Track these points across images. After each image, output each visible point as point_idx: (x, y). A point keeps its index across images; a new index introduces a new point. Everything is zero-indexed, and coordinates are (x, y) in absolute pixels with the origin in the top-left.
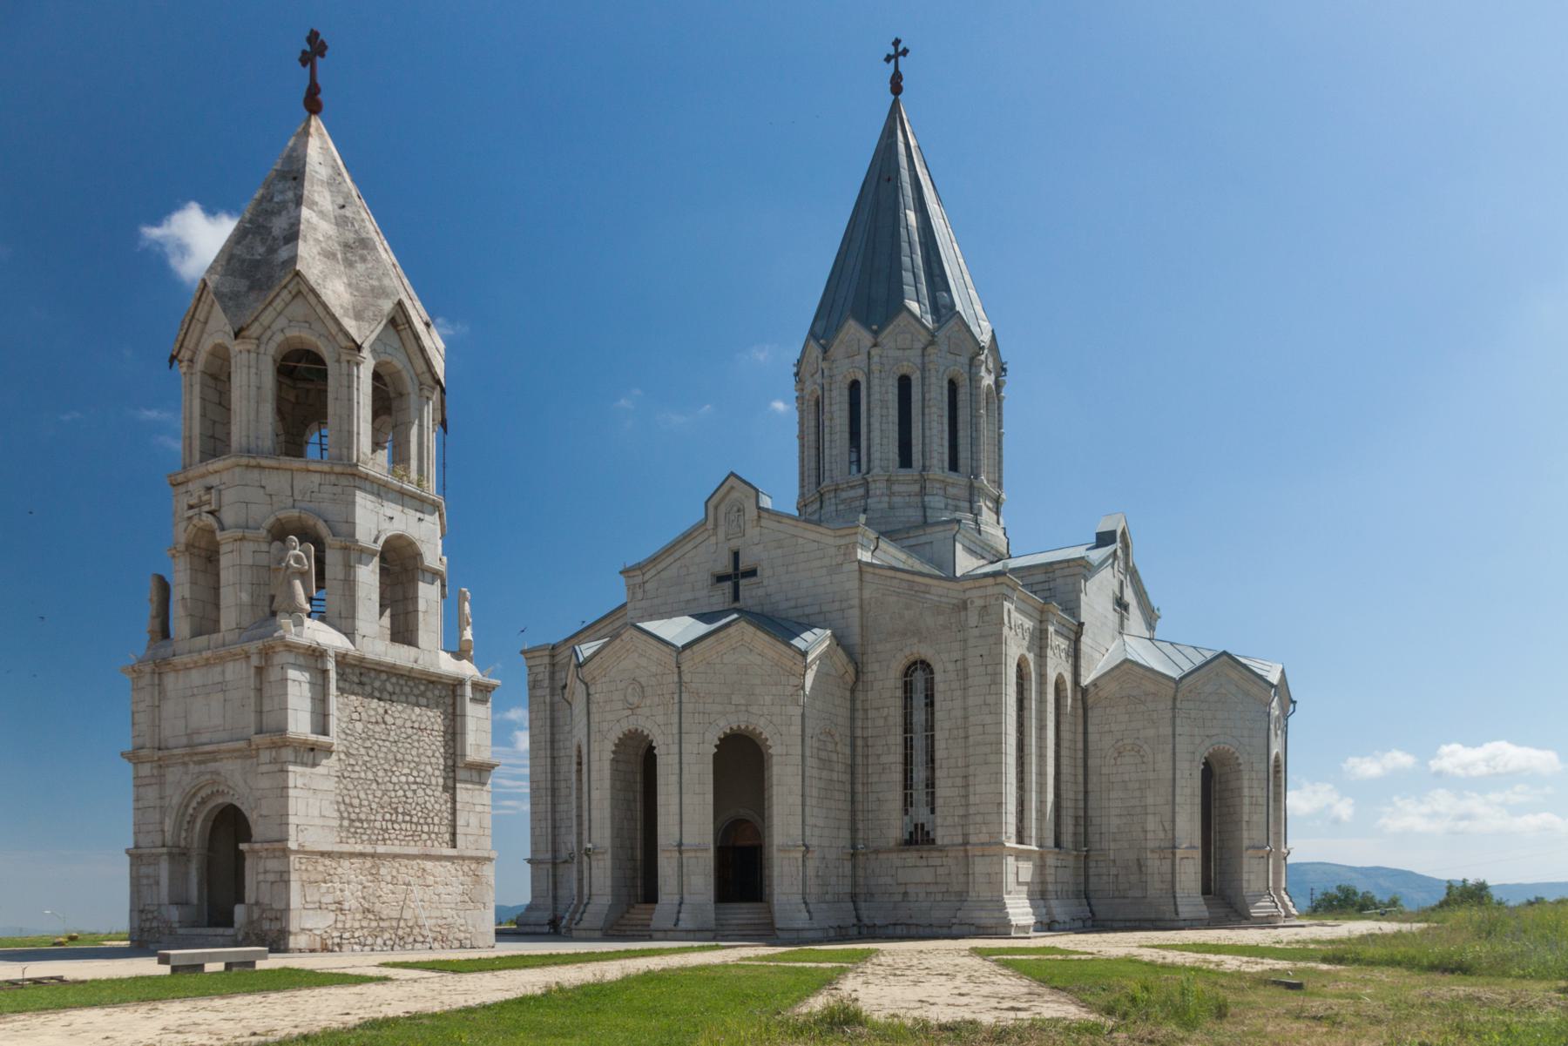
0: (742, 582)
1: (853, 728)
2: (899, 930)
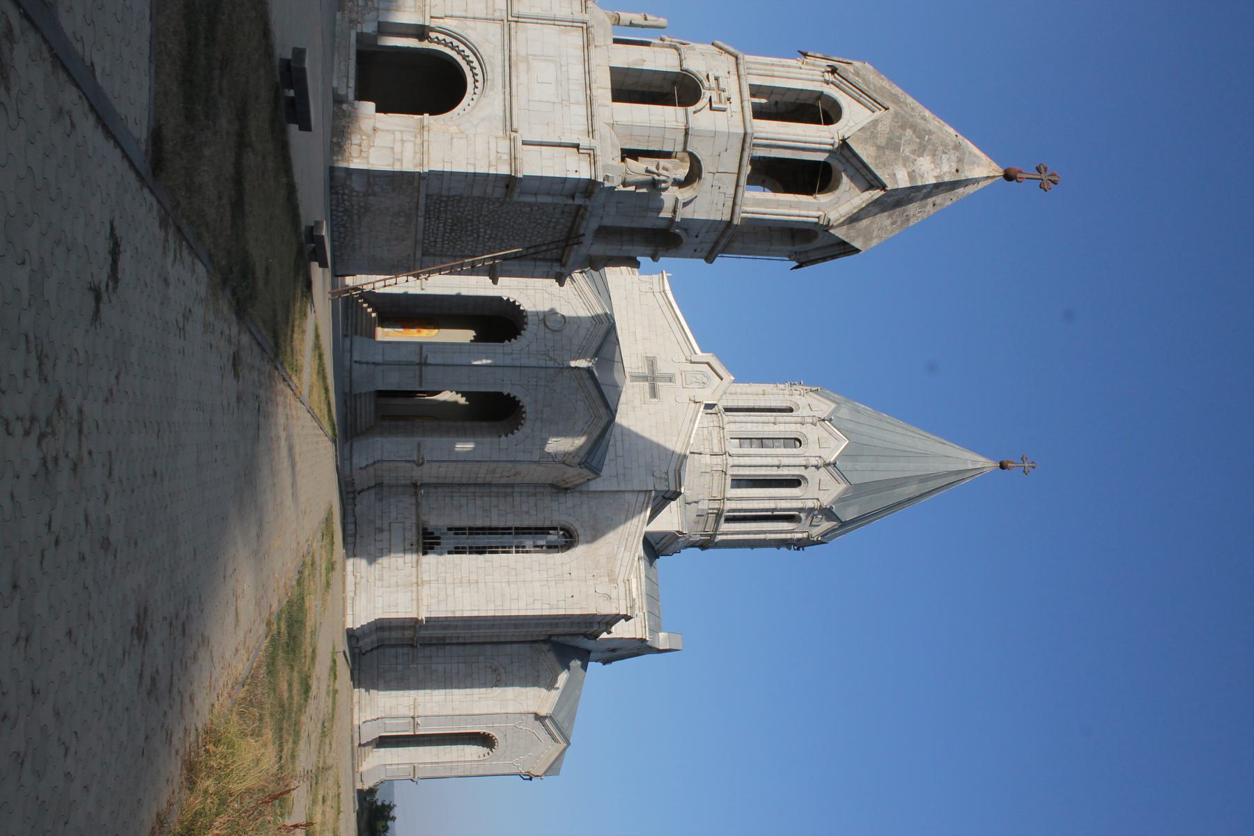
1: (521, 485)
2: (351, 527)
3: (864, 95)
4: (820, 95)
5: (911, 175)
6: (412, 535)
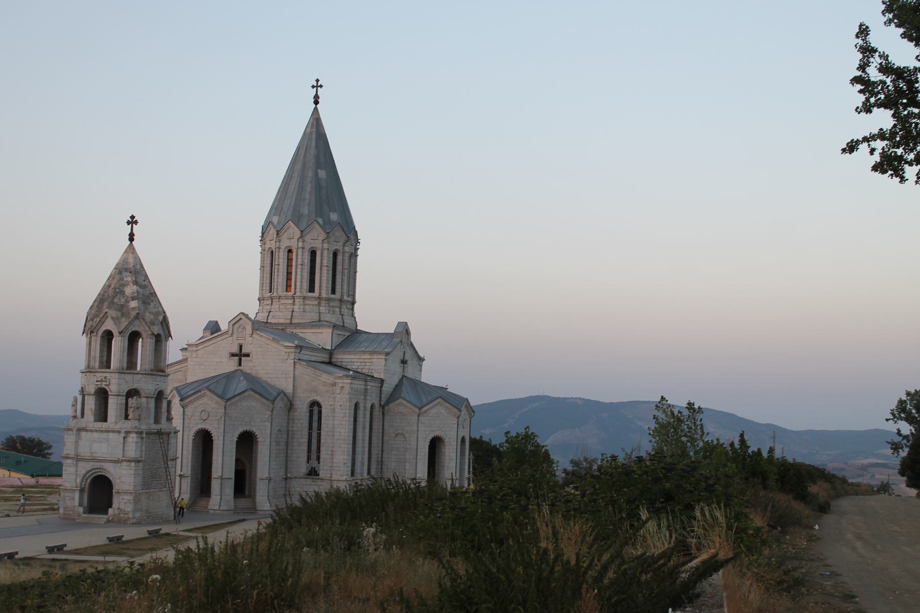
0: (243, 358)
1: (288, 427)
3: (102, 322)
4: (102, 337)
5: (133, 299)
6: (309, 481)
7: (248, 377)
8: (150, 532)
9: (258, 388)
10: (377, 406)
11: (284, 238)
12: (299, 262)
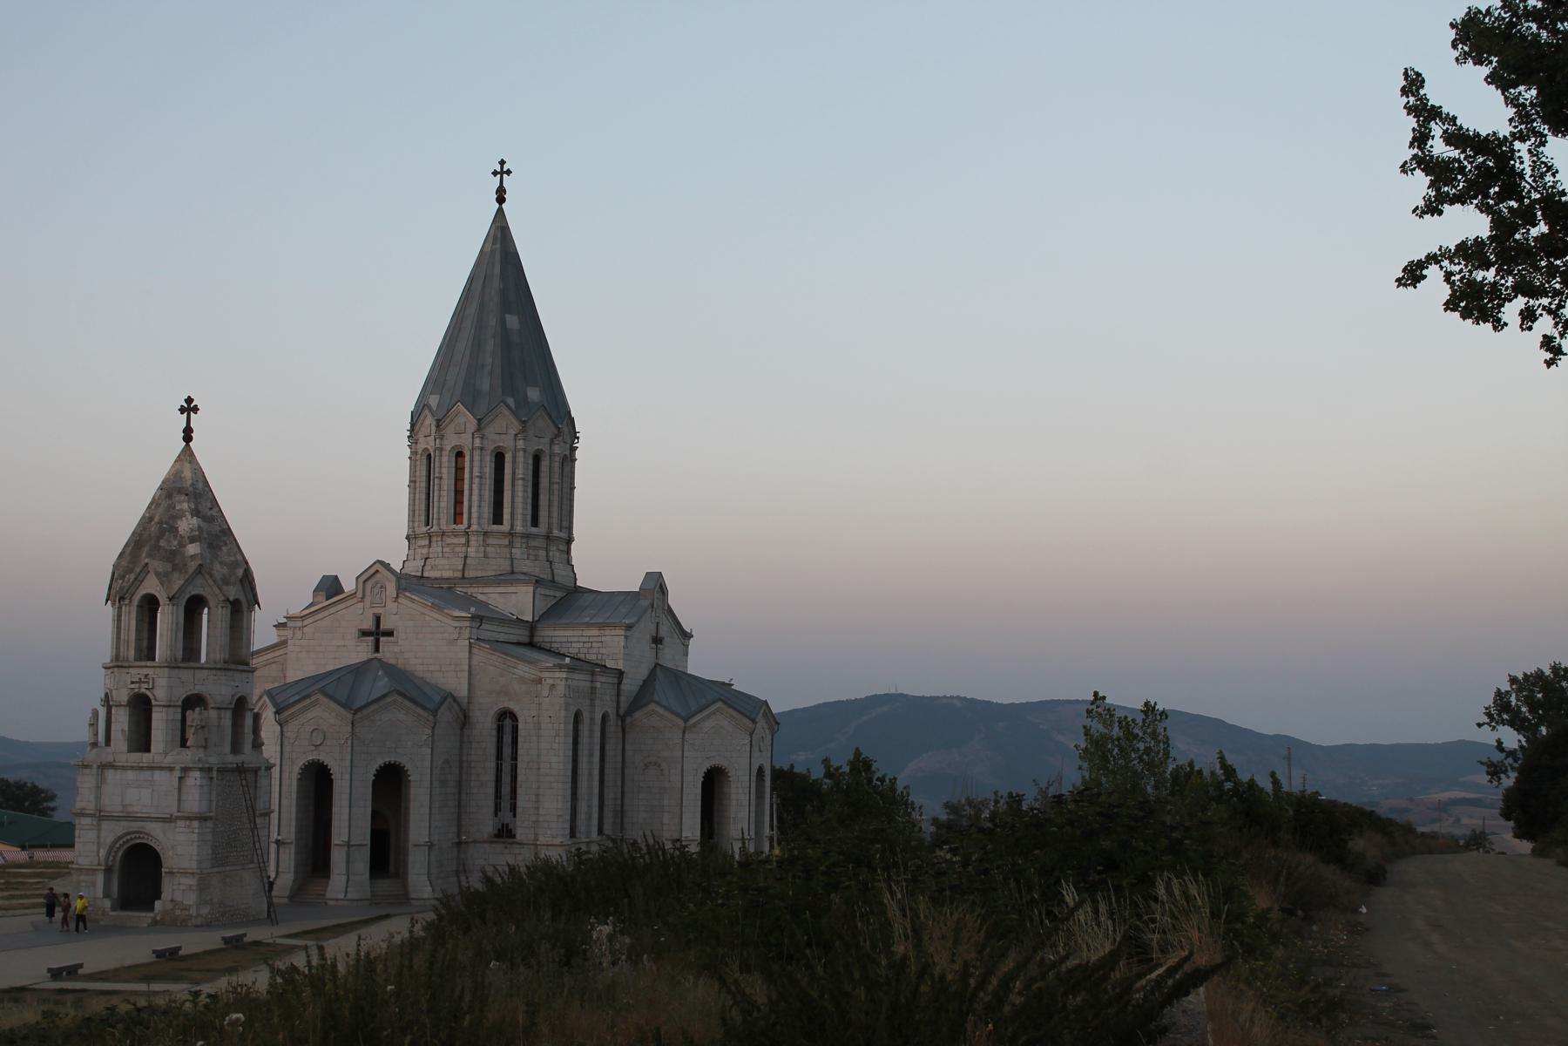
1: (461, 755)
3: (139, 580)
4: (139, 606)
5: (192, 540)
7: (392, 671)
8: (226, 940)
9: (408, 689)
10: (612, 716)
11: (449, 431)
12: (476, 472)
